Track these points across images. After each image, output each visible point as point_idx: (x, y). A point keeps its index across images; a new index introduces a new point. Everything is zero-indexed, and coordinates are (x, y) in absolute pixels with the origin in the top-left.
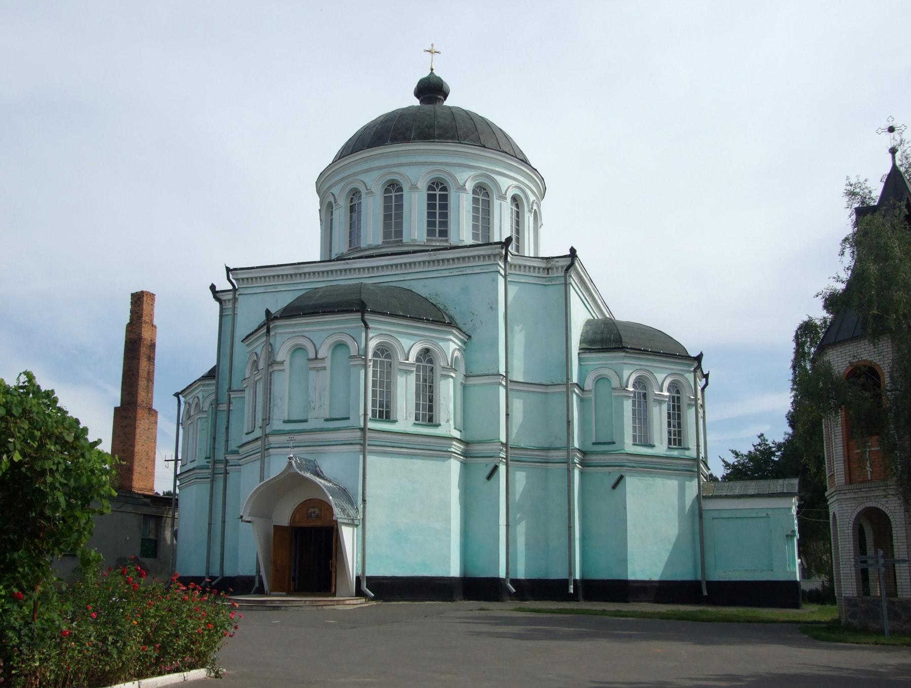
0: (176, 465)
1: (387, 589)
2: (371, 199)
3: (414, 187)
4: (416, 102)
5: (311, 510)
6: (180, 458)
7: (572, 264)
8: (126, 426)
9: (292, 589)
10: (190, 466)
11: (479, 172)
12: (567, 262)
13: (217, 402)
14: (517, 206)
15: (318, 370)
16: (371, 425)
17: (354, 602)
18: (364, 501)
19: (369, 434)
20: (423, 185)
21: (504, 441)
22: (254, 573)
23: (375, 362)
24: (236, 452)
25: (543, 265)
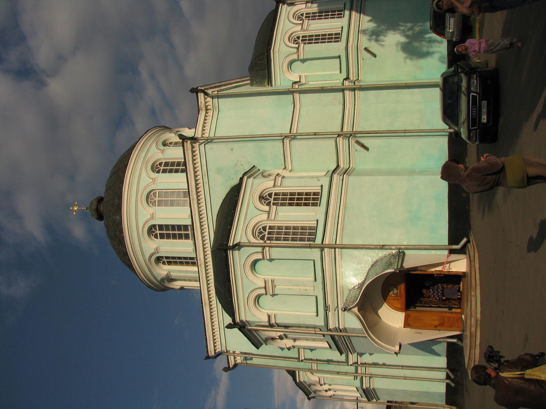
2: (161, 248)
4: (103, 221)
9: (459, 311)
11: (144, 169)
15: (274, 287)
19: (327, 242)
20: (151, 210)
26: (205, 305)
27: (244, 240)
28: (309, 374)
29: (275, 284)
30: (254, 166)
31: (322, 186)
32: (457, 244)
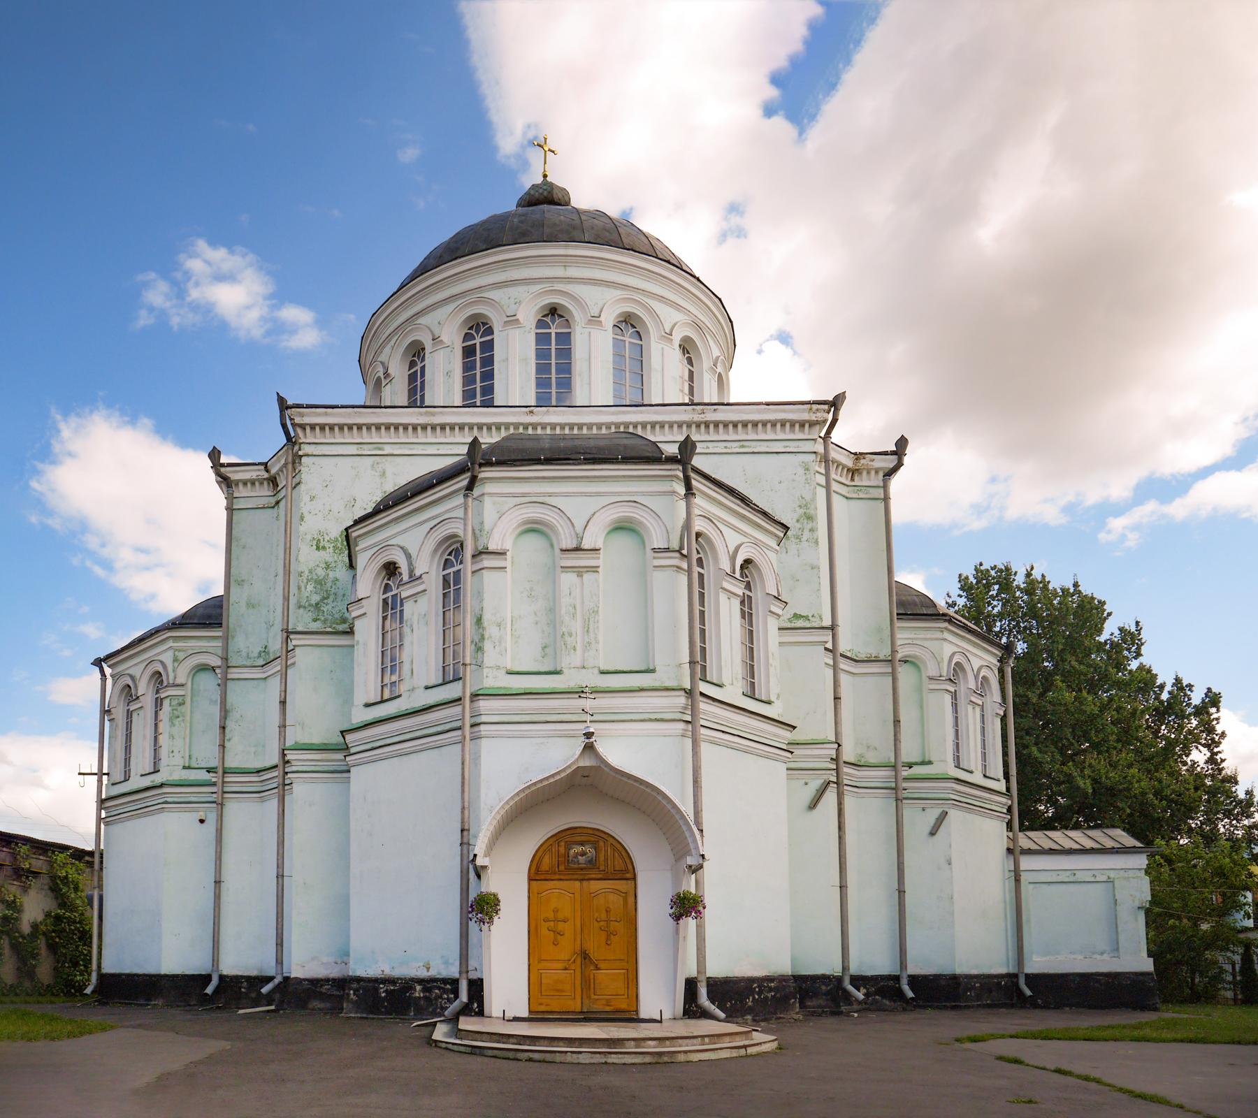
0: (100, 781)
2: (517, 331)
25: (849, 462)
26: (426, 413)
29: (586, 576)
31: (769, 703)
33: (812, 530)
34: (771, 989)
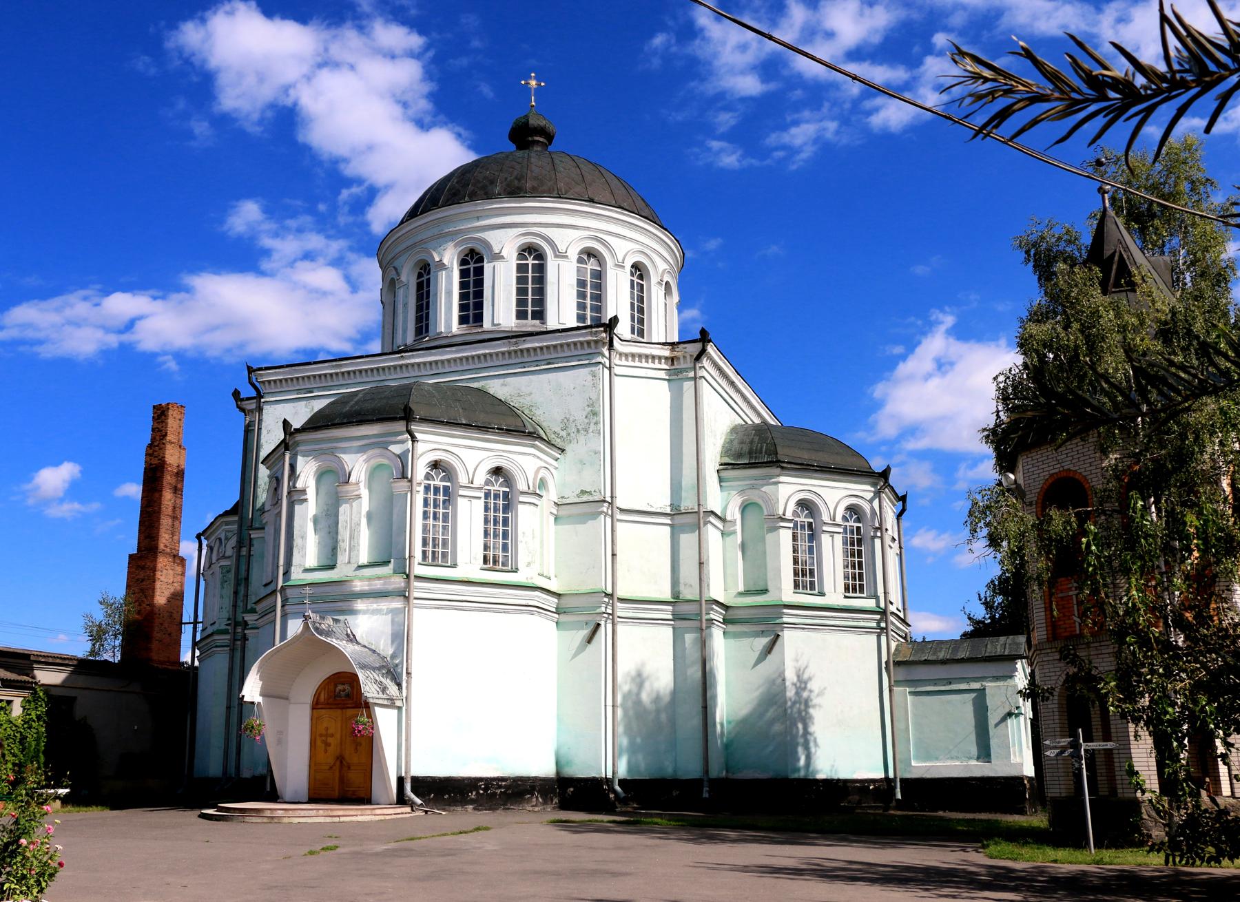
1: (441, 792)
3: (498, 257)
5: (340, 687)
6: (200, 619)
7: (703, 351)
8: (143, 580)
10: (206, 634)
11: (587, 233)
12: (694, 349)
13: (240, 544)
14: (641, 277)
16: (419, 570)
17: (399, 810)
18: (408, 674)
21: (609, 591)
22: (265, 771)
23: (427, 488)
24: (253, 611)
25: (666, 352)
27: (420, 447)
28: (233, 542)
30: (563, 451)
32: (412, 791)
33: (596, 423)
34: (500, 787)
